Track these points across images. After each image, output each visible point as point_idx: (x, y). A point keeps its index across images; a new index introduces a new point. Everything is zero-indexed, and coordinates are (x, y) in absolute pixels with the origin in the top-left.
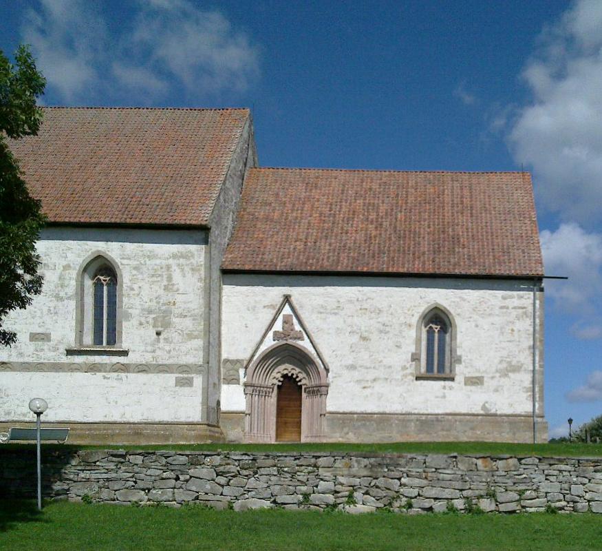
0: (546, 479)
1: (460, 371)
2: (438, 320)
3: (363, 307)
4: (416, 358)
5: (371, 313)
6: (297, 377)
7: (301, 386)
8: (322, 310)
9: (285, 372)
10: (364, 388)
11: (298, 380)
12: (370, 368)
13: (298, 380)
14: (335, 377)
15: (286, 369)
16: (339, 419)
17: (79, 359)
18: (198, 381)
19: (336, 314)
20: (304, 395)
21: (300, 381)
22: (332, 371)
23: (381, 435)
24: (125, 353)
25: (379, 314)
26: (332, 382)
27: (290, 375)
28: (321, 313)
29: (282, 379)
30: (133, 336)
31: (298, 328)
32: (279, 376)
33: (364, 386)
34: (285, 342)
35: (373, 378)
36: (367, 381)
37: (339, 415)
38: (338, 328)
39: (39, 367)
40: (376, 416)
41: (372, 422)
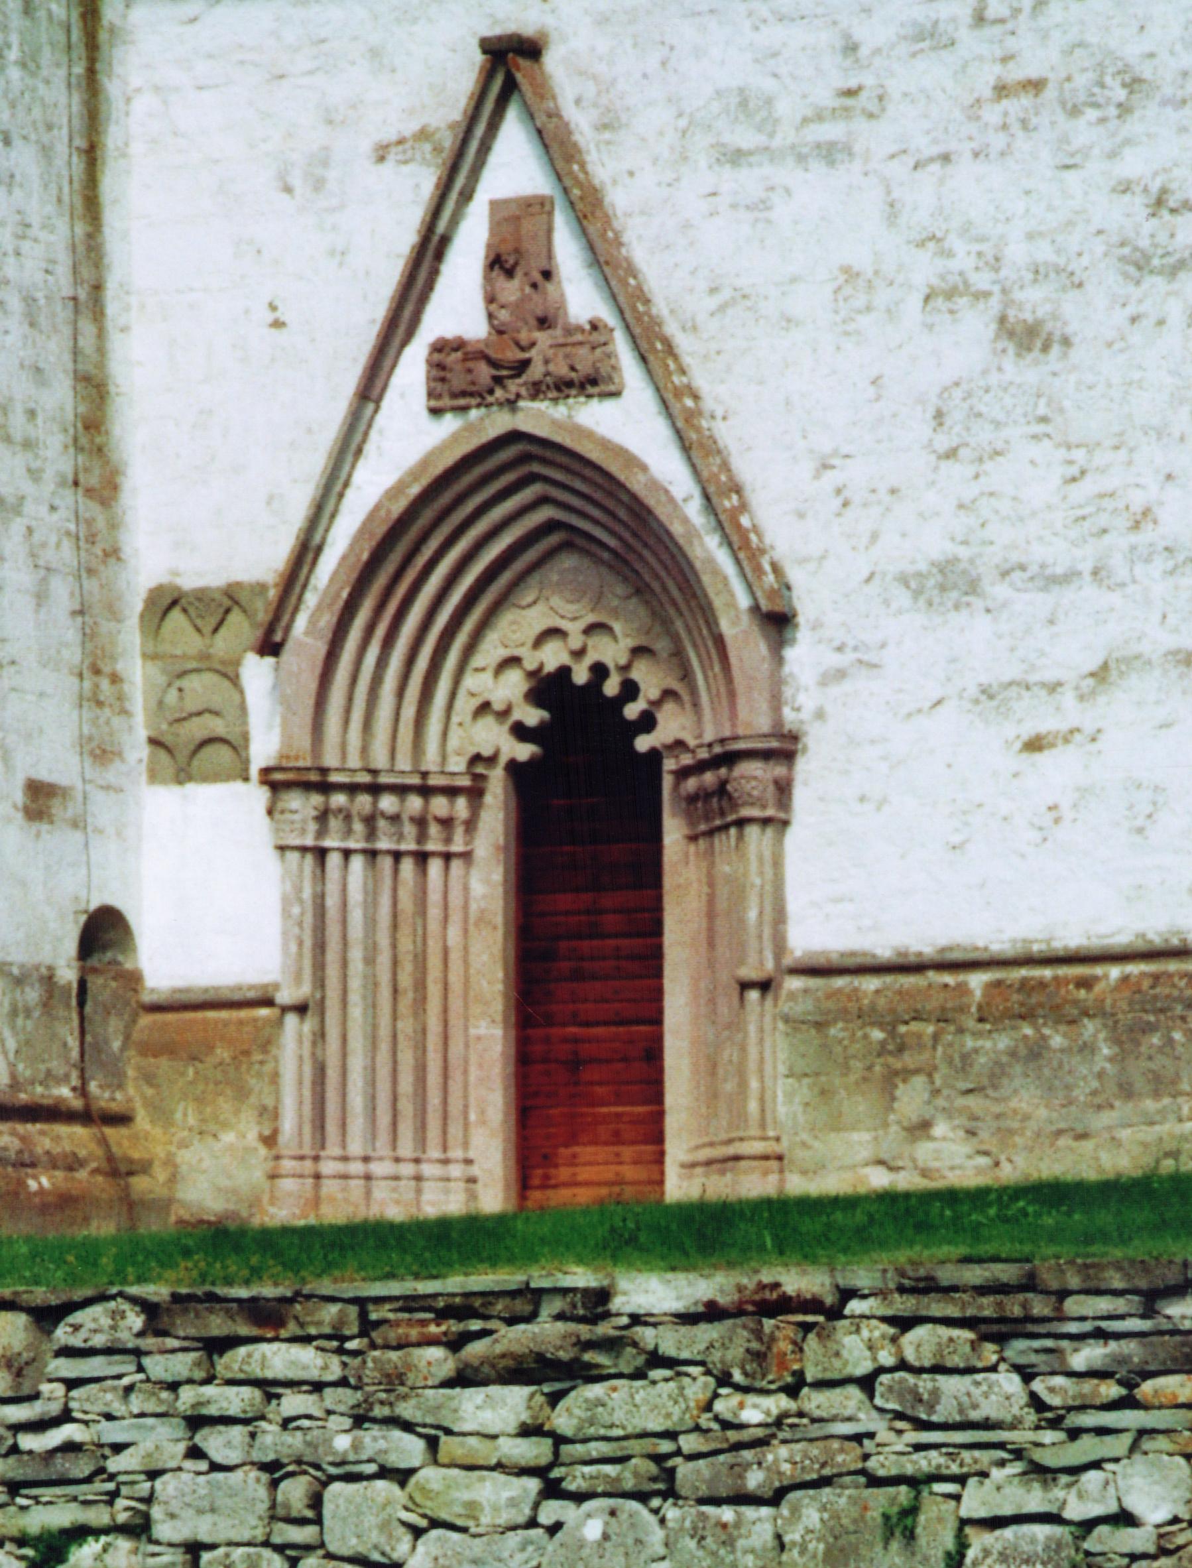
0: (195, 1453)
3: (1016, 73)
5: (1074, 111)
6: (630, 690)
7: (655, 756)
8: (745, 138)
9: (552, 657)
10: (1035, 745)
11: (632, 711)
12: (1068, 577)
13: (632, 711)
14: (840, 674)
15: (554, 632)
16: (866, 1016)
19: (830, 153)
20: (673, 831)
21: (647, 722)
22: (816, 626)
23: (1149, 1134)
25: (1124, 109)
26: (820, 715)
27: (581, 676)
28: (736, 157)
29: (533, 716)
32: (513, 686)
33: (1028, 730)
34: (498, 423)
35: (1093, 664)
36: (1053, 688)
37: (871, 984)
38: (850, 274)
40: (1115, 972)
41: (1090, 1027)
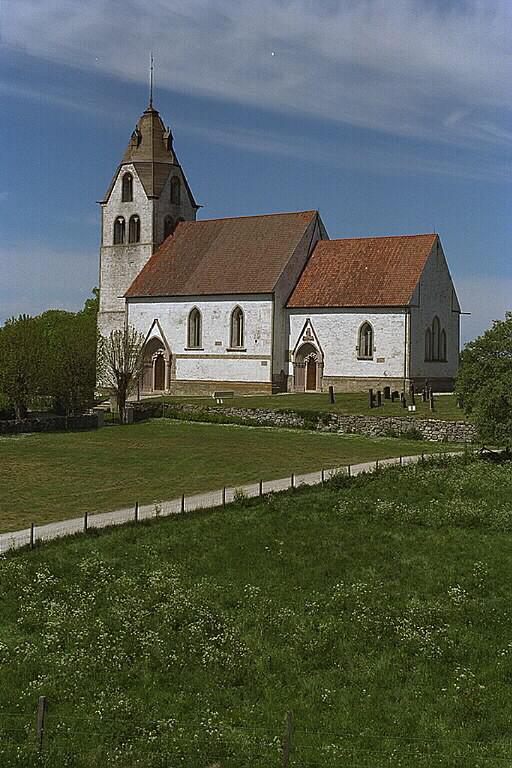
1: (375, 354)
2: (366, 329)
4: (359, 349)
17: (230, 353)
18: (269, 362)
24: (245, 351)
30: (248, 342)
31: (312, 335)
39: (218, 357)
